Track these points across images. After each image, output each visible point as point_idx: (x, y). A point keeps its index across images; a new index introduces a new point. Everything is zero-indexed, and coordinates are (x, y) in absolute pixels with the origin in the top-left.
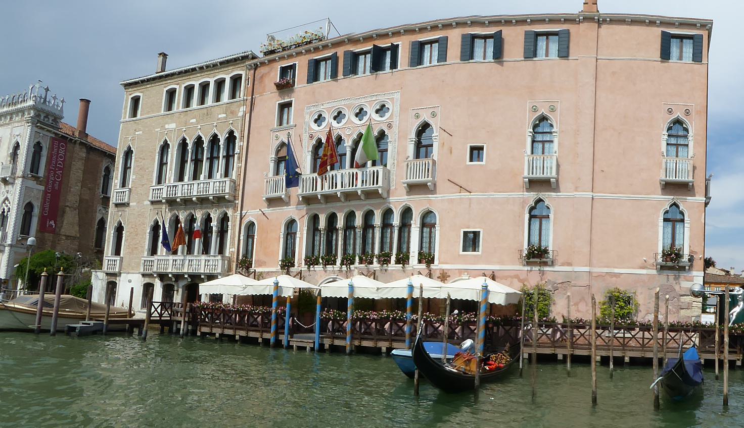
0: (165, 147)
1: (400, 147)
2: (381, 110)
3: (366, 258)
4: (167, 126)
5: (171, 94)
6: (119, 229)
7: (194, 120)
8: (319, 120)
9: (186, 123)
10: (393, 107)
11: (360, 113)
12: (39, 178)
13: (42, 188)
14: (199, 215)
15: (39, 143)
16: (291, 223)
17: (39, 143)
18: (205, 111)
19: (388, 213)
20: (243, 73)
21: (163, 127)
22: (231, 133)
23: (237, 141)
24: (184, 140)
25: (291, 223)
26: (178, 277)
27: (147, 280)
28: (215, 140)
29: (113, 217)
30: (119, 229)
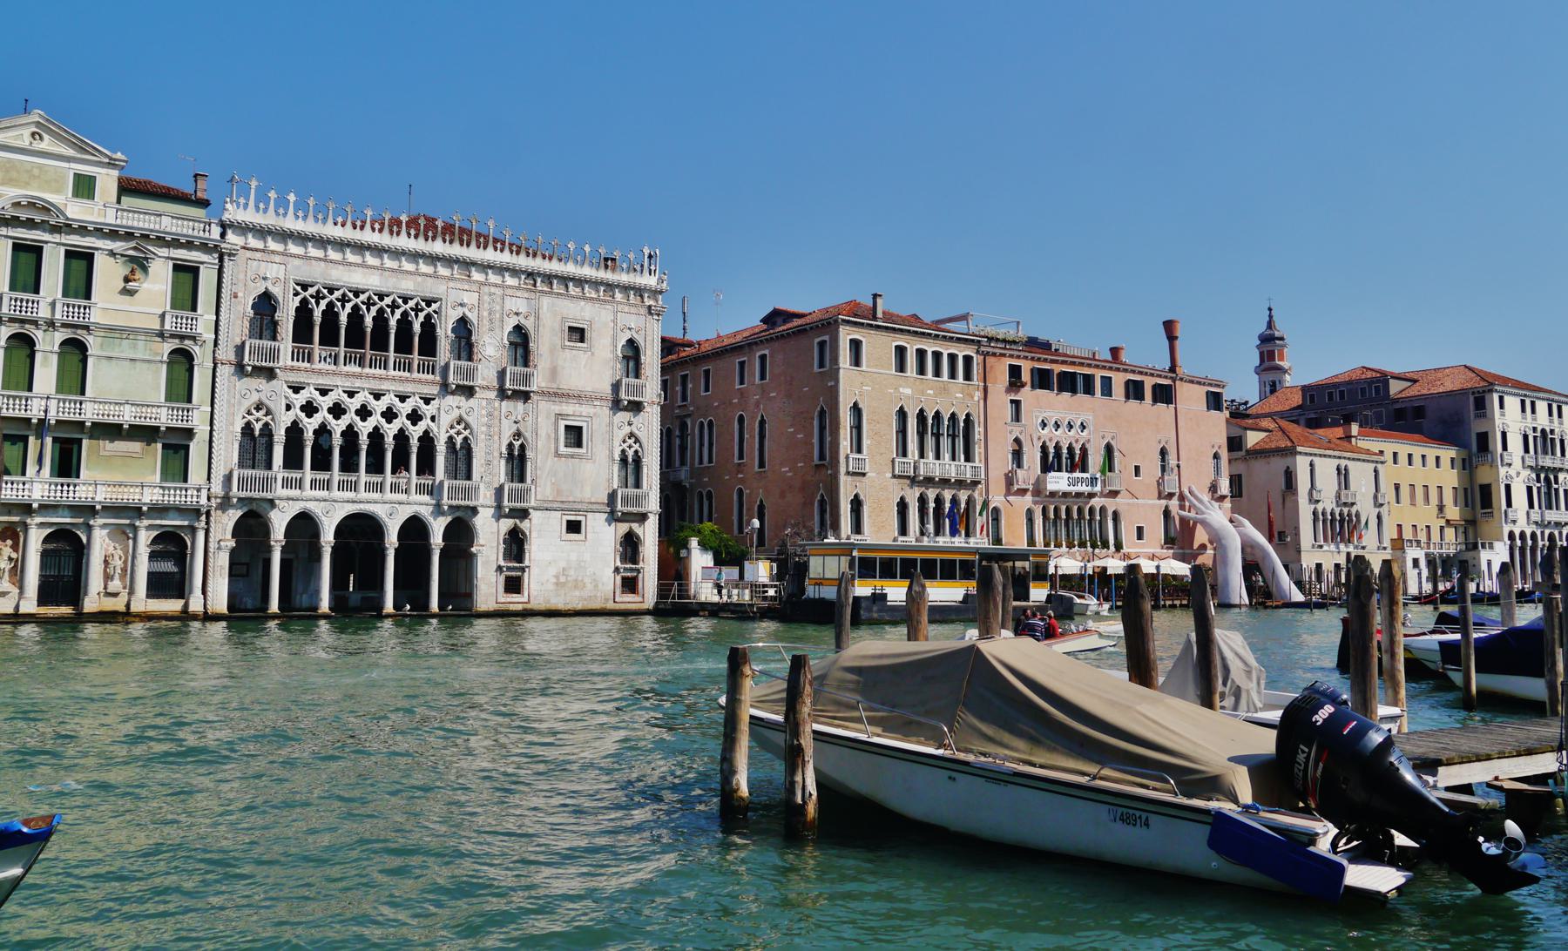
0: (902, 414)
1: (1095, 460)
2: (1083, 427)
3: (1082, 545)
5: (901, 351)
6: (857, 504)
8: (1044, 425)
9: (923, 393)
10: (1090, 427)
14: (947, 495)
16: (1030, 513)
19: (1091, 510)
22: (968, 415)
25: (1030, 513)
29: (847, 489)
30: (857, 504)
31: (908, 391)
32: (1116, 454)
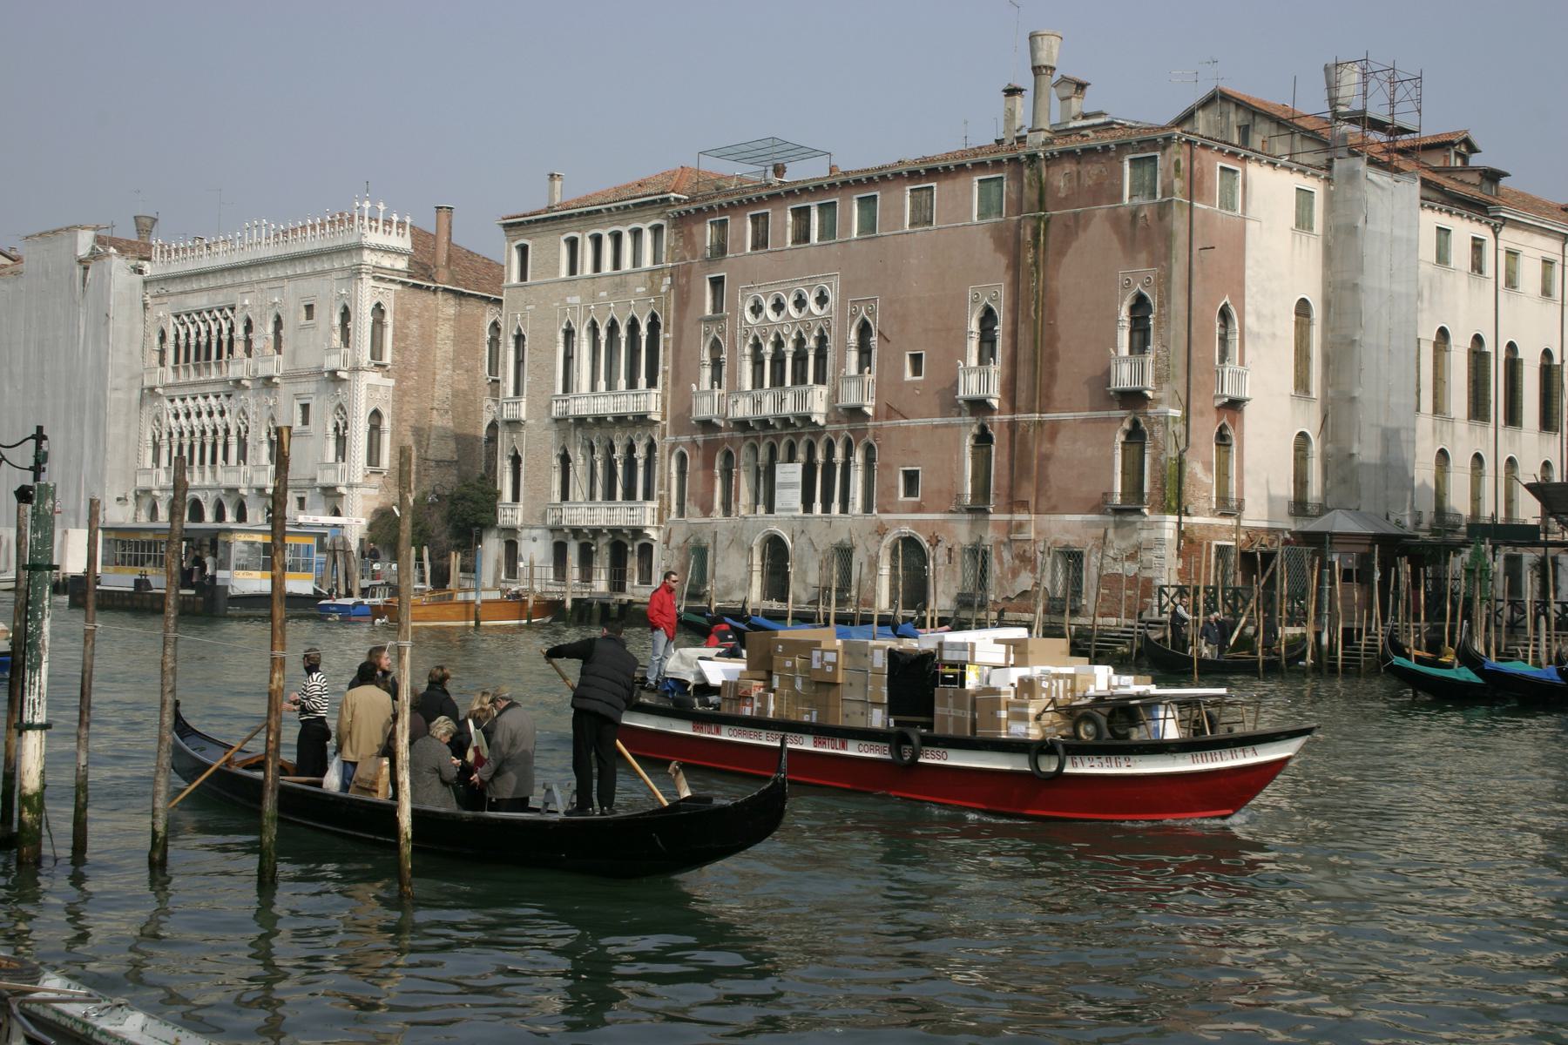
0: (569, 333)
4: (569, 300)
7: (604, 294)
8: (757, 309)
11: (800, 303)
12: (384, 366)
13: (391, 382)
15: (378, 305)
17: (378, 305)
18: (617, 279)
20: (664, 223)
21: (563, 300)
22: (654, 317)
23: (661, 331)
24: (594, 323)
26: (596, 532)
27: (558, 537)
28: (633, 326)
31: (576, 300)
32: (874, 339)
